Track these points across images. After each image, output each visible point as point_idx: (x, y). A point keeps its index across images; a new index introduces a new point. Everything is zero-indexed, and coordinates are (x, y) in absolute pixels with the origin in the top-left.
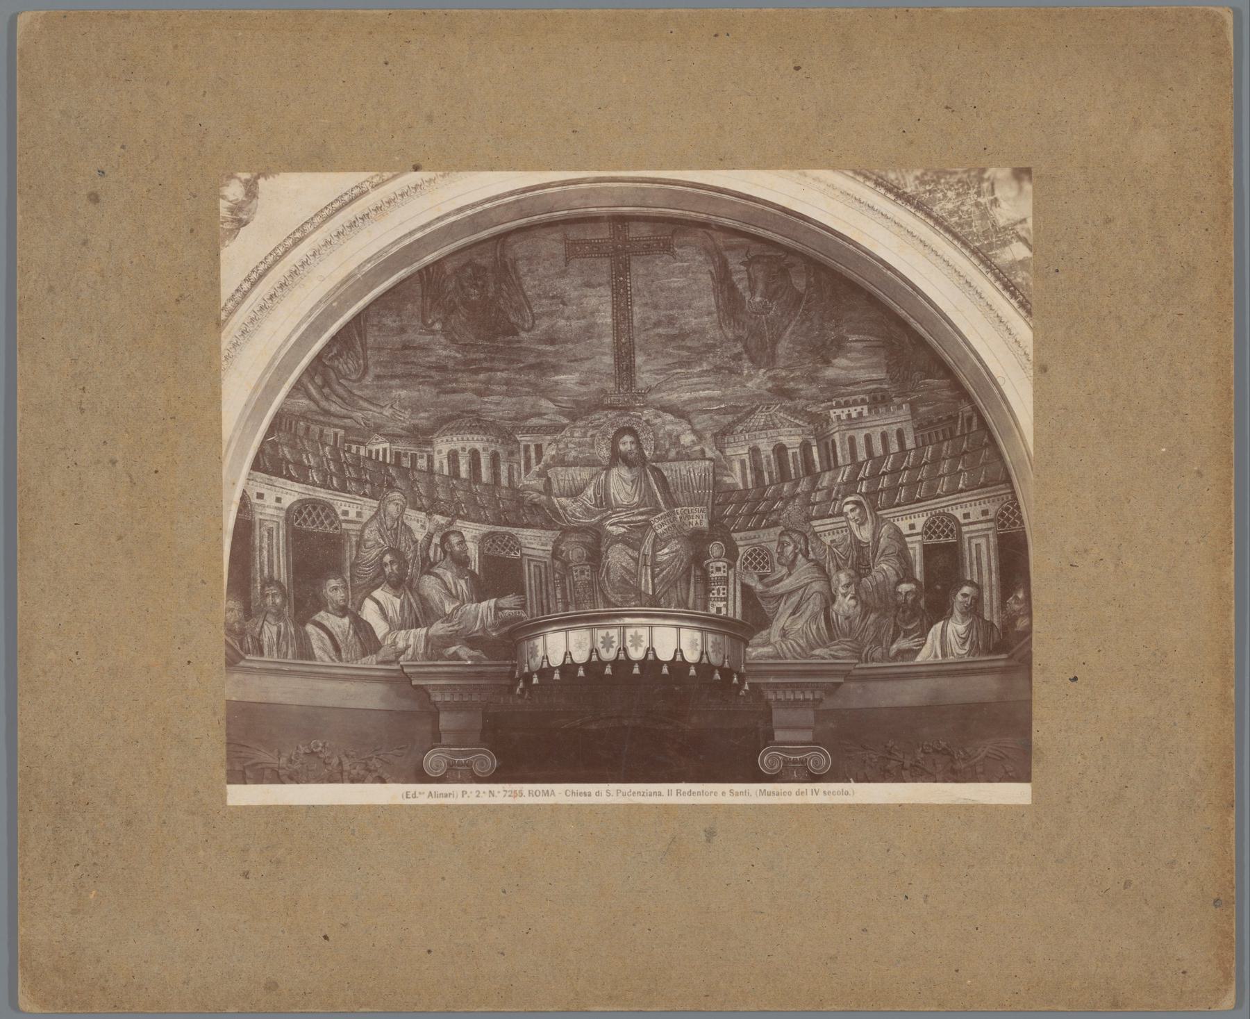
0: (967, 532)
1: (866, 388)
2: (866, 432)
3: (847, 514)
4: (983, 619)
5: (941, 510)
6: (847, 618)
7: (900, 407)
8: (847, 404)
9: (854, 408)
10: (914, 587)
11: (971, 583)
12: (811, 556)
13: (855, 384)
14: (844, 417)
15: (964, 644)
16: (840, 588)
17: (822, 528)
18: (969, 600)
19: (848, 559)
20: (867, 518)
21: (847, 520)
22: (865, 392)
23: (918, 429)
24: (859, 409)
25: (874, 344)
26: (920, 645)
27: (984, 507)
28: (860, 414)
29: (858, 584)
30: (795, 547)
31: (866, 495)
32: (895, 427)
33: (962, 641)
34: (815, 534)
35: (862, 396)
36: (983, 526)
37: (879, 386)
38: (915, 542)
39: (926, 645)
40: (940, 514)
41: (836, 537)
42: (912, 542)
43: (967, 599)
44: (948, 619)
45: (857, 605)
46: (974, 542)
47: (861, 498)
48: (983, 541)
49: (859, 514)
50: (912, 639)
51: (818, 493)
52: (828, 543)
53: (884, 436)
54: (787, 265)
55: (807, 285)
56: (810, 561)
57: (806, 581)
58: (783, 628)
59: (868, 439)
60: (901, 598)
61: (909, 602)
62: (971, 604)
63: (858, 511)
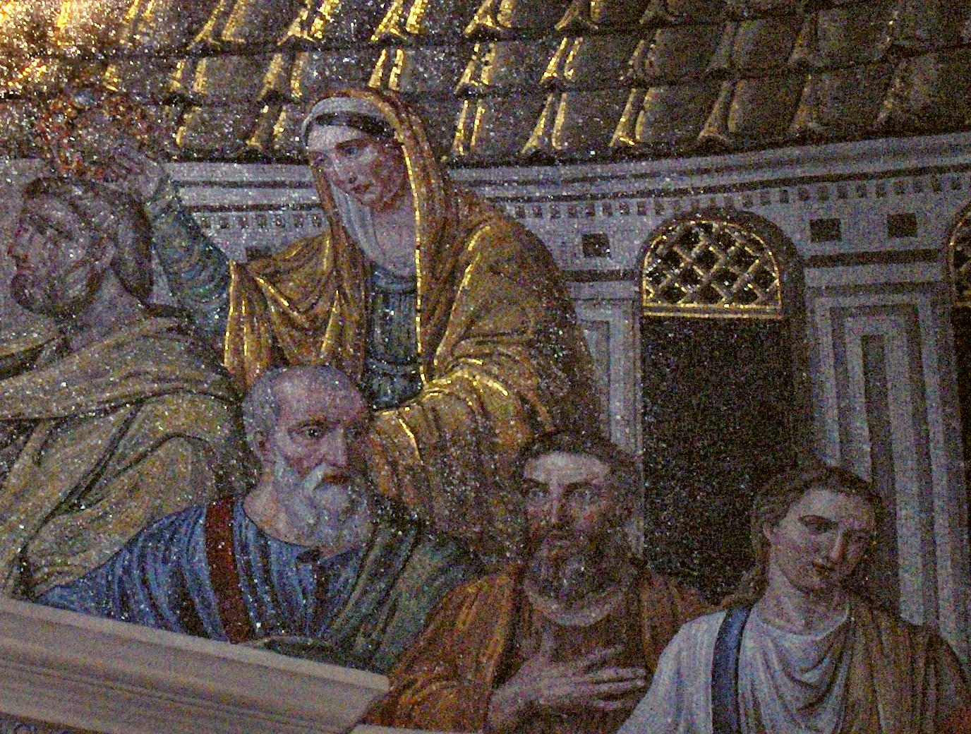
0: (832, 290)
3: (321, 158)
4: (898, 619)
5: (720, 199)
6: (313, 555)
10: (598, 469)
11: (844, 480)
12: (162, 293)
15: (811, 708)
16: (280, 436)
17: (211, 197)
18: (833, 543)
19: (319, 331)
20: (405, 186)
21: (324, 183)
26: (624, 694)
27: (895, 204)
29: (360, 429)
30: (96, 242)
31: (406, 102)
33: (805, 696)
34: (183, 214)
36: (899, 272)
38: (614, 302)
39: (649, 696)
40: (712, 212)
41: (270, 235)
42: (594, 302)
43: (823, 538)
44: (748, 606)
45: (350, 511)
46: (856, 327)
47: (387, 108)
48: (890, 328)
49: (375, 167)
50: (589, 669)
51: (203, 63)
52: (241, 256)
56: (152, 311)
57: (134, 387)
58: (23, 557)
60: (545, 509)
61: (581, 523)
62: (843, 555)
63: (369, 155)
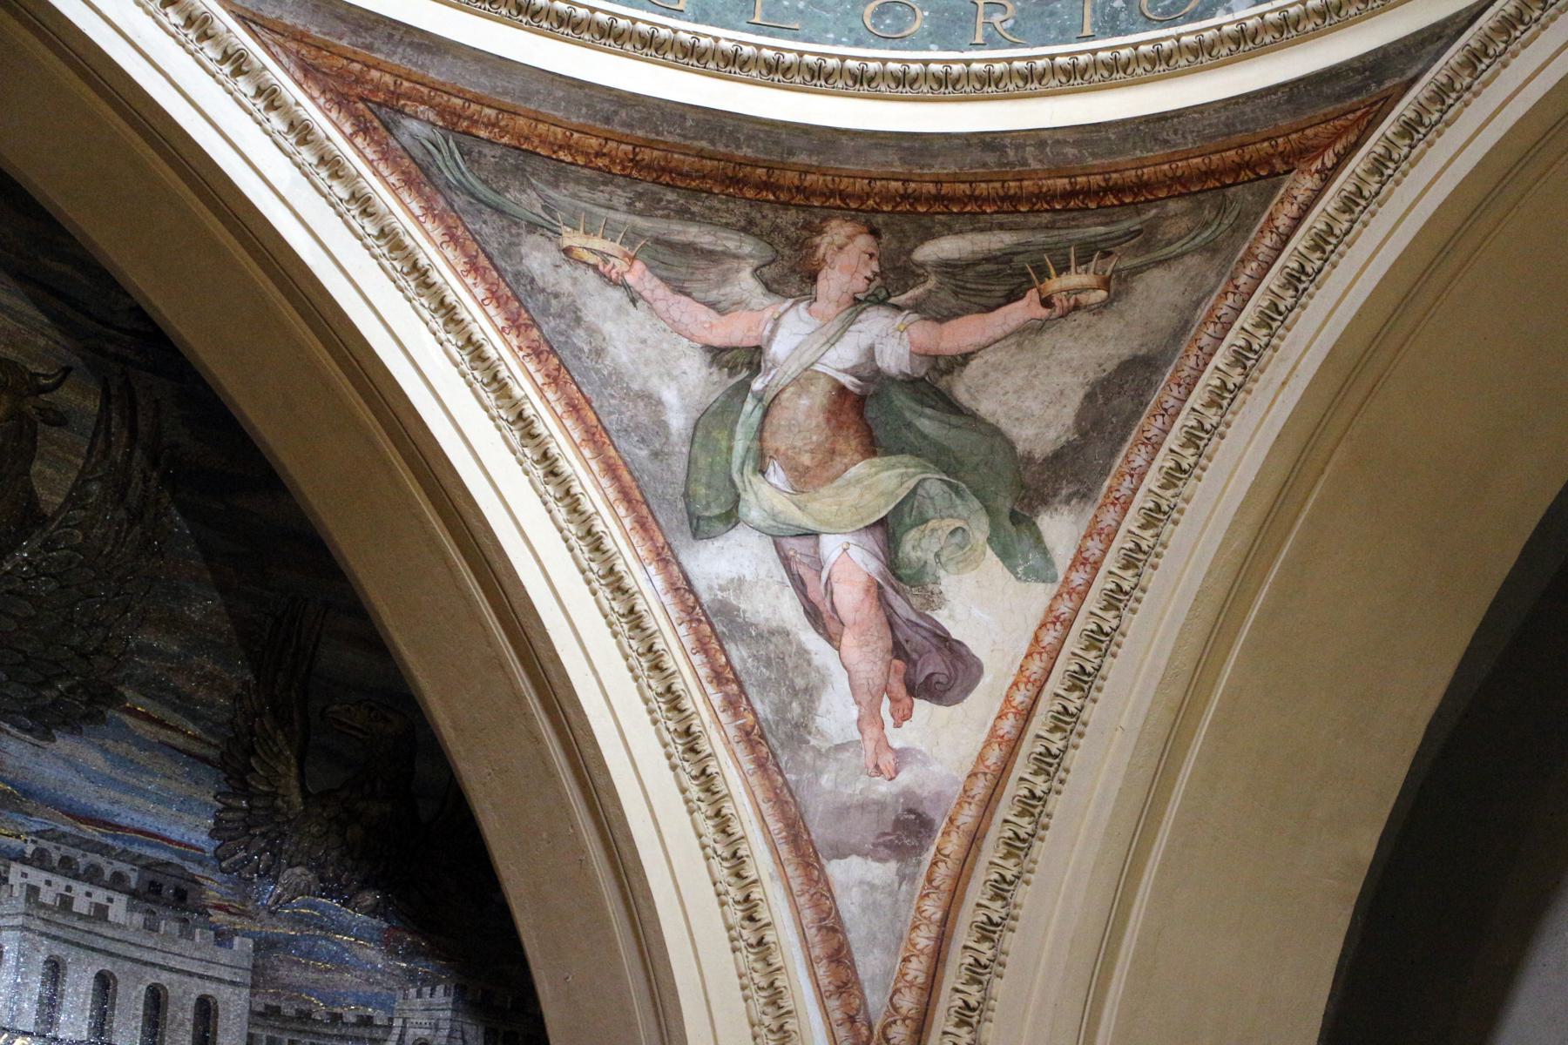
1: (135, 849)
2: (106, 965)
7: (223, 938)
8: (66, 867)
9: (87, 887)
13: (106, 824)
14: (47, 897)
22: (134, 859)
23: (260, 1014)
24: (100, 896)
25: (196, 748)
28: (101, 913)
32: (197, 989)
35: (124, 867)
37: (176, 860)
53: (156, 1000)
54: (41, 411)
55: (69, 498)
59: (104, 983)
